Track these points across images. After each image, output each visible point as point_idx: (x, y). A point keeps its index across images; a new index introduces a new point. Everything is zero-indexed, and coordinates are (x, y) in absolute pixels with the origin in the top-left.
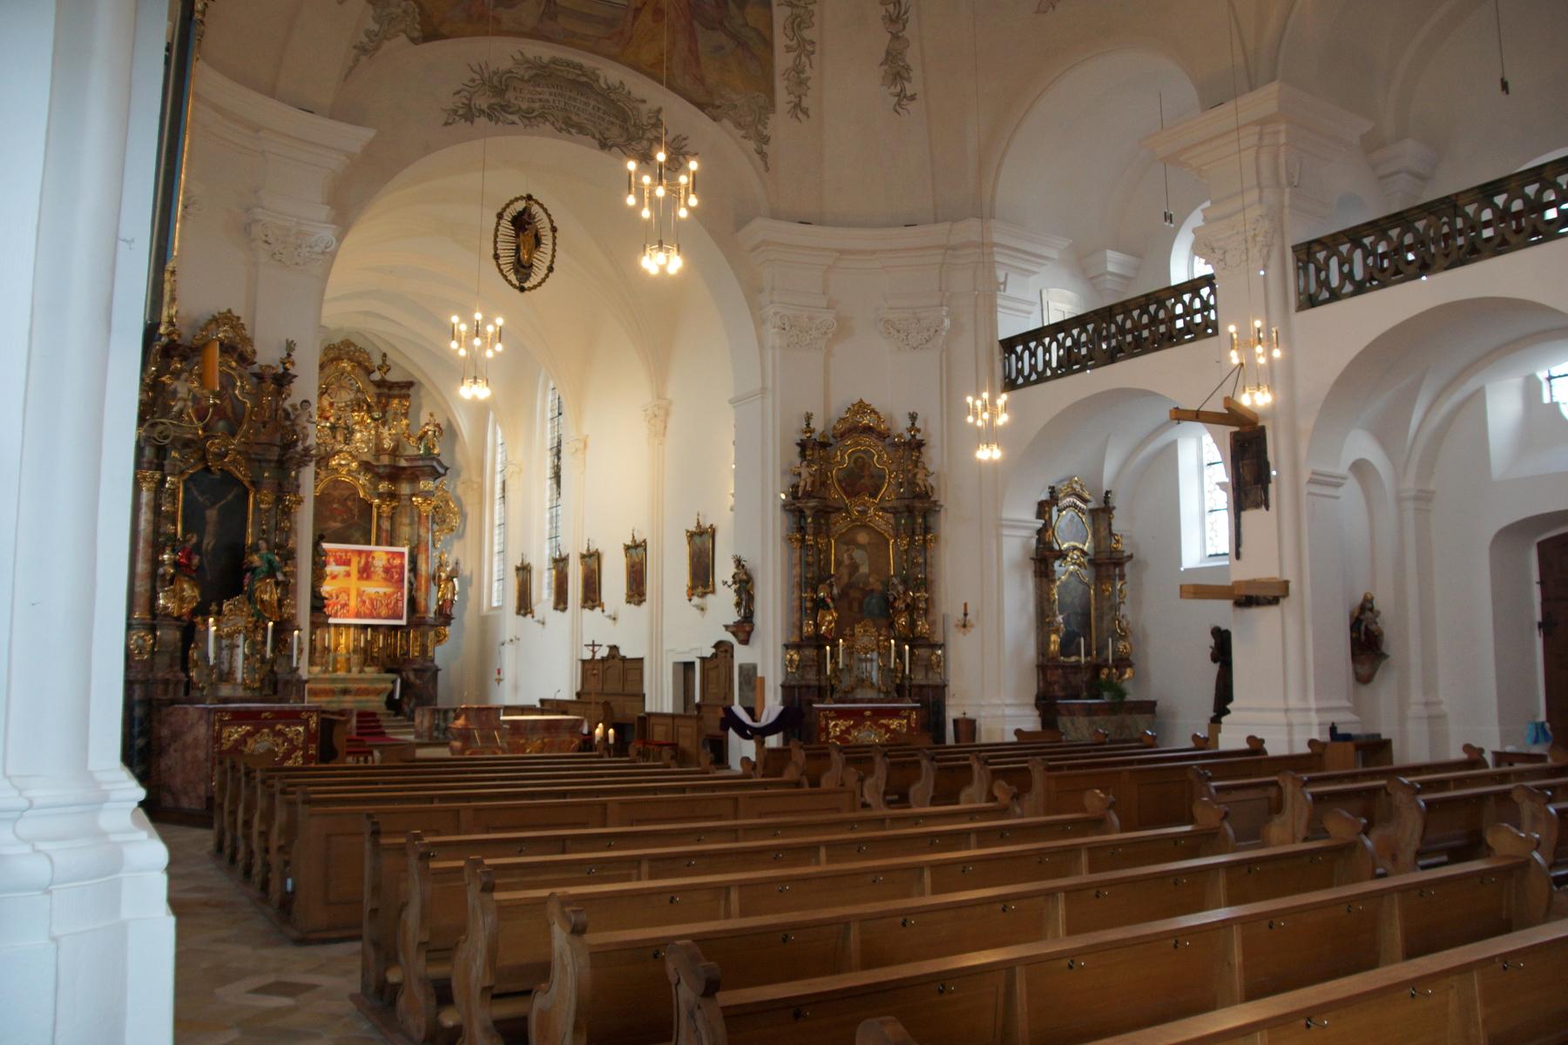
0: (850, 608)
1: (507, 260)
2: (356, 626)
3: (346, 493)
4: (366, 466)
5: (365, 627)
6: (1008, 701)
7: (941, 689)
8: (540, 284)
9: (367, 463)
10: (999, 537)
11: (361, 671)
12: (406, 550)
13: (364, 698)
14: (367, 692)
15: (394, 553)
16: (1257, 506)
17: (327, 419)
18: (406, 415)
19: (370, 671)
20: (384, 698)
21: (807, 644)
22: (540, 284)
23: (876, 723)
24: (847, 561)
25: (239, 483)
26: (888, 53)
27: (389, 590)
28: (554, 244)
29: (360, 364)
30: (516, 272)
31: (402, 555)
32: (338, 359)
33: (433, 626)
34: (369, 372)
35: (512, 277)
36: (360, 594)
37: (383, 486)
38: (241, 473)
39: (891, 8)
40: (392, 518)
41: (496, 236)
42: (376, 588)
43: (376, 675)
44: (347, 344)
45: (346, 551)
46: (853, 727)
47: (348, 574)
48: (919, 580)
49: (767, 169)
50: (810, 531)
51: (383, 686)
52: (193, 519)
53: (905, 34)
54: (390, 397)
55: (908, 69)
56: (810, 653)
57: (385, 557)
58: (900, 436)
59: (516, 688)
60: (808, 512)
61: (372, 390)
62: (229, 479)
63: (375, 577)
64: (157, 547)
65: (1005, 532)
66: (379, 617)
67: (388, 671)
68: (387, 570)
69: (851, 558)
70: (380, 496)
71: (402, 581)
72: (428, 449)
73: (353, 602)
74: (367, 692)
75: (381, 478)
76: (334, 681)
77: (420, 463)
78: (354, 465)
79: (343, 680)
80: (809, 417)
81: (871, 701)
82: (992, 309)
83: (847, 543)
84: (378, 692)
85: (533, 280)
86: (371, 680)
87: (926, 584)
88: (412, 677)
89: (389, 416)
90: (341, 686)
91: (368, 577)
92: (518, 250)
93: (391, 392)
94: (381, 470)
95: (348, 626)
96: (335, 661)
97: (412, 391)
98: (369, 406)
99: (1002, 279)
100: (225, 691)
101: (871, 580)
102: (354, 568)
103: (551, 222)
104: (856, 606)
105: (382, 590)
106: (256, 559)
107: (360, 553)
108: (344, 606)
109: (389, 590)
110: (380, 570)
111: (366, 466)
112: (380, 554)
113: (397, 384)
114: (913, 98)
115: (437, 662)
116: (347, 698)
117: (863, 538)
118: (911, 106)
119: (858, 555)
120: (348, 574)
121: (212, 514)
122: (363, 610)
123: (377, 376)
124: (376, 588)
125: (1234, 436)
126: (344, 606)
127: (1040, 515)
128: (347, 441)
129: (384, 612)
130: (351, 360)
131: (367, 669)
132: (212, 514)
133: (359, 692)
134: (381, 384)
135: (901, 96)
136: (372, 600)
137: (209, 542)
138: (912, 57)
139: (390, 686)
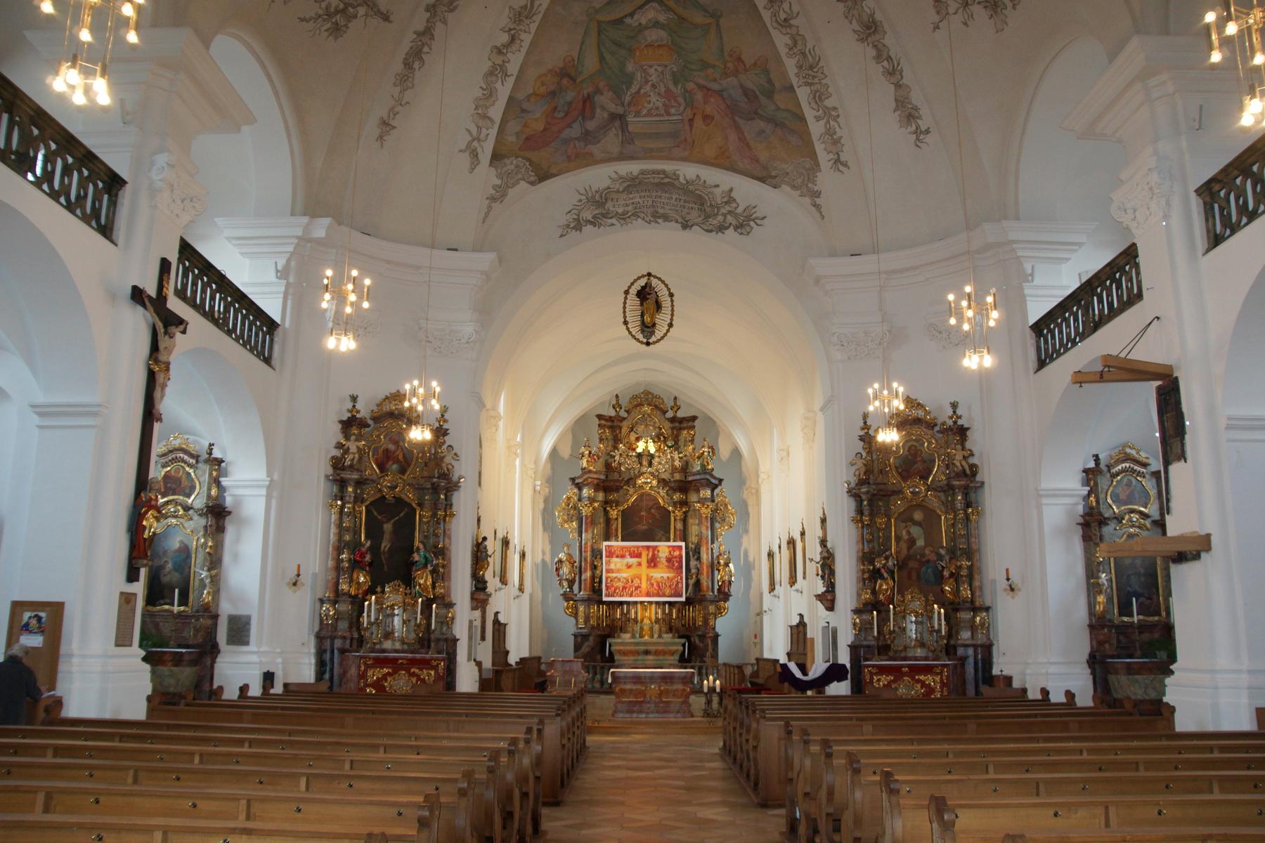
1: (635, 327)
2: (657, 603)
3: (651, 503)
4: (663, 482)
5: (664, 603)
6: (1052, 660)
8: (662, 338)
10: (1039, 507)
11: (660, 636)
16: (1179, 460)
18: (692, 441)
19: (667, 637)
20: (677, 657)
21: (871, 607)
22: (662, 338)
23: (913, 678)
24: (905, 537)
25: (410, 505)
26: (896, 100)
27: (671, 575)
28: (672, 306)
29: (656, 406)
30: (643, 331)
32: (641, 405)
33: (712, 602)
34: (665, 412)
35: (640, 337)
36: (649, 578)
37: (677, 497)
38: (410, 496)
39: (885, 64)
40: (685, 521)
41: (624, 308)
42: (661, 574)
44: (647, 393)
46: (894, 681)
47: (640, 564)
48: (966, 552)
49: (823, 217)
50: (866, 513)
52: (374, 530)
53: (904, 81)
54: (681, 429)
55: (916, 109)
57: (667, 550)
58: (944, 424)
59: (771, 649)
60: (864, 497)
61: (668, 425)
62: (400, 502)
63: (660, 565)
64: (339, 550)
65: (1044, 501)
66: (664, 595)
67: (680, 637)
68: (669, 560)
69: (909, 533)
70: (675, 504)
72: (703, 466)
73: (644, 585)
75: (675, 490)
76: (637, 644)
77: (698, 477)
78: (655, 483)
79: (645, 644)
82: (1022, 300)
84: (672, 653)
85: (658, 334)
86: (666, 644)
87: (970, 553)
89: (681, 443)
90: (642, 648)
91: (655, 566)
92: (642, 316)
93: (679, 425)
95: (650, 603)
96: (642, 628)
97: (697, 423)
99: (1029, 271)
100: (388, 645)
101: (927, 552)
102: (644, 560)
103: (669, 289)
105: (665, 575)
106: (416, 557)
107: (648, 548)
109: (671, 575)
110: (664, 560)
112: (663, 548)
114: (927, 132)
115: (717, 630)
116: (650, 657)
117: (918, 516)
118: (928, 138)
120: (640, 564)
121: (388, 527)
122: (651, 590)
123: (670, 414)
124: (661, 574)
125: (1159, 389)
126: (637, 588)
127: (1086, 482)
128: (650, 464)
129: (668, 591)
130: (649, 405)
131: (665, 636)
132: (388, 527)
134: (673, 420)
135: (918, 132)
137: (385, 545)
138: (916, 98)
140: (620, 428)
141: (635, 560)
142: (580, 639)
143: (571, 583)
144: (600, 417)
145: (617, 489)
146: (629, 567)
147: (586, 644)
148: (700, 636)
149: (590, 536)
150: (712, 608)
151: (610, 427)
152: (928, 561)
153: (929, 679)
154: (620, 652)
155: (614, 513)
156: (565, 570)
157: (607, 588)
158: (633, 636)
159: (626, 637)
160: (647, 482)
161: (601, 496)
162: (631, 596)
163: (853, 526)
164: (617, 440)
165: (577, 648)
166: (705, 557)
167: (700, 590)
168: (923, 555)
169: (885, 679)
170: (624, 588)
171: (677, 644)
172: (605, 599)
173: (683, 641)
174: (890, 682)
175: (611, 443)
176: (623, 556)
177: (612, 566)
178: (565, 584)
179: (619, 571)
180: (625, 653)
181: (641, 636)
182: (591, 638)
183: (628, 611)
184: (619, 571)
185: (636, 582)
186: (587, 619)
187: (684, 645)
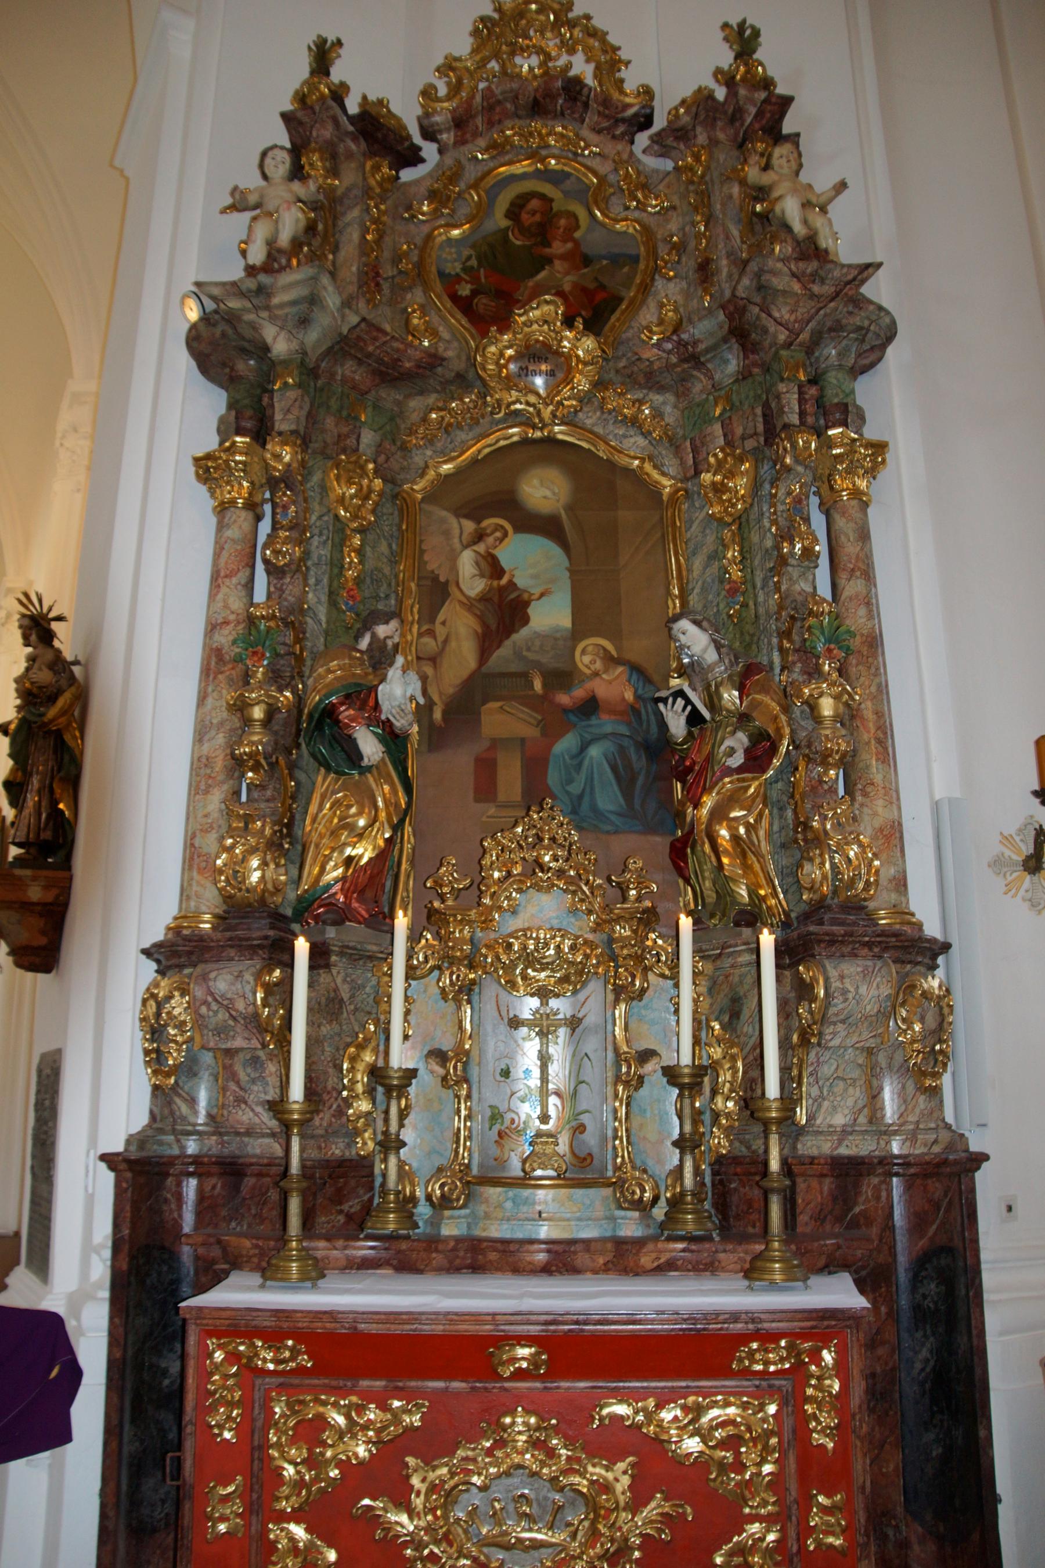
0: (486, 788)
7: (948, 1178)
24: (470, 579)
56: (235, 983)
80: (323, 56)
81: (563, 1260)
83: (475, 510)
101: (585, 659)
104: (510, 778)
117: (543, 490)
119: (528, 558)
152: (590, 706)
153: (692, 1424)
163: (200, 502)
168: (562, 677)
169: (354, 1429)
174: (392, 1451)
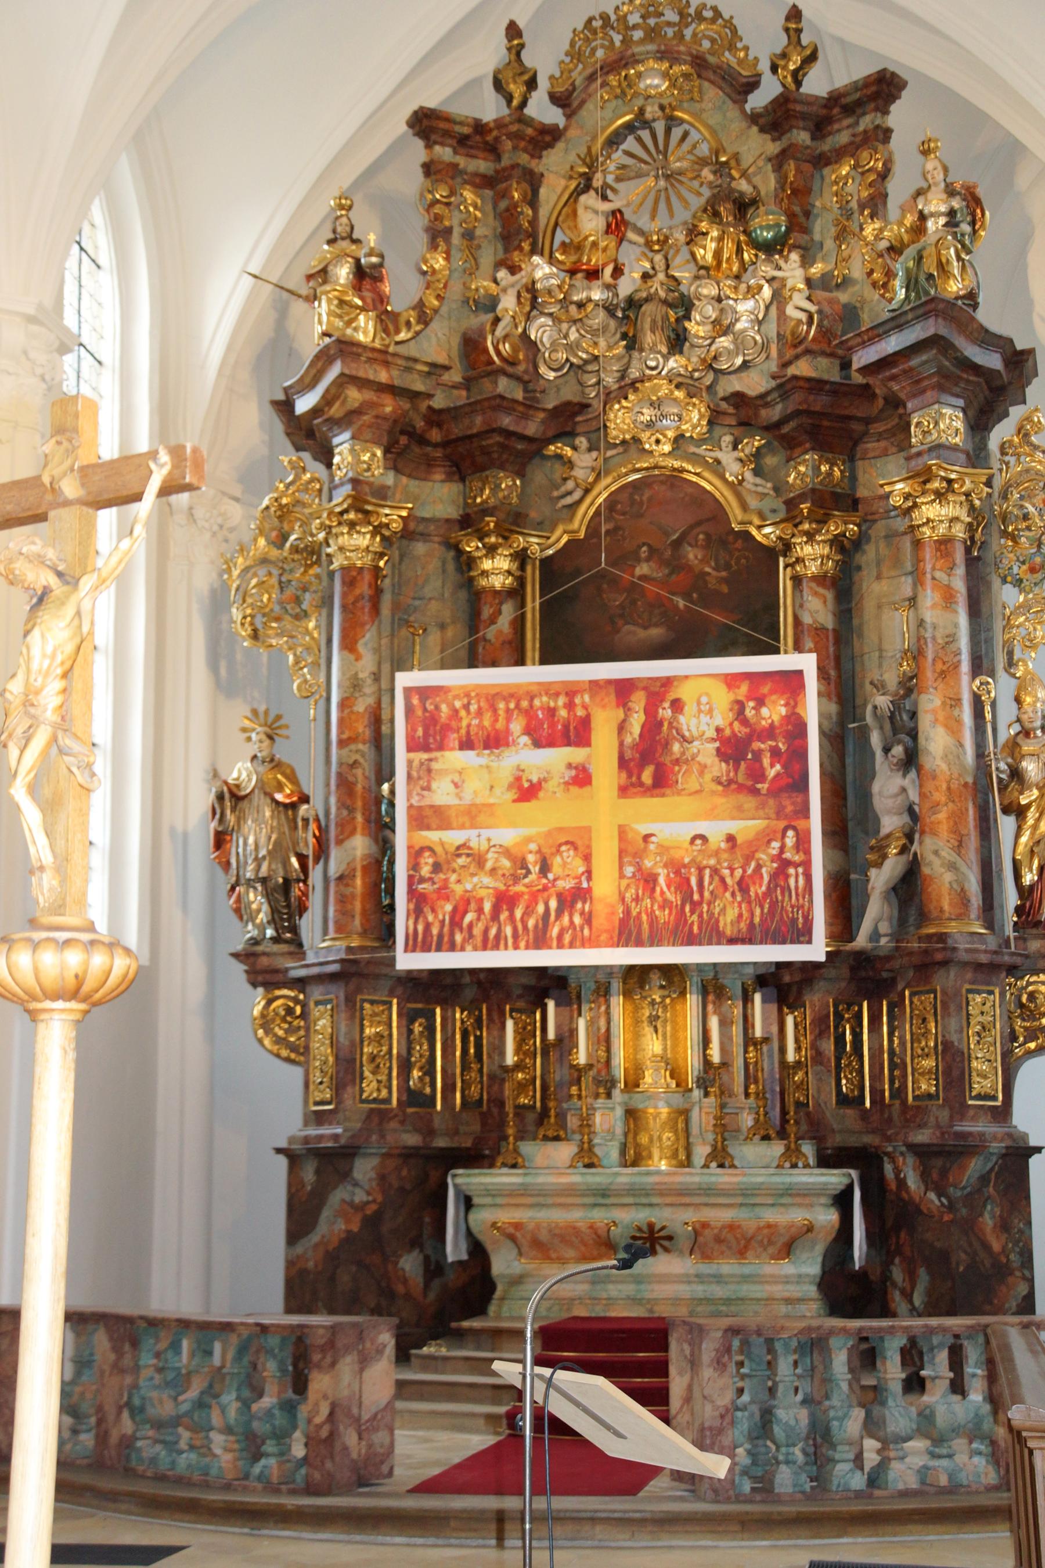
2: (713, 984)
3: (677, 523)
4: (738, 413)
9: (738, 399)
11: (720, 1157)
12: (807, 663)
13: (728, 1267)
14: (738, 1242)
15: (755, 678)
17: (593, 274)
19: (759, 1160)
20: (809, 1265)
29: (699, 63)
31: (793, 681)
33: (990, 970)
36: (630, 848)
37: (804, 471)
40: (842, 585)
42: (695, 822)
43: (760, 1177)
45: (571, 691)
47: (582, 777)
51: (797, 1216)
54: (822, 161)
57: (722, 698)
61: (755, 147)
66: (713, 935)
67: (825, 1161)
68: (733, 748)
71: (801, 785)
73: (605, 886)
74: (738, 1242)
76: (603, 1195)
77: (893, 344)
86: (747, 1196)
88: (913, 1182)
89: (822, 229)
91: (662, 783)
94: (775, 413)
97: (901, 116)
98: (743, 207)
102: (602, 754)
105: (717, 830)
107: (623, 689)
108: (575, 896)
109: (745, 828)
110: (706, 752)
111: (738, 413)
112: (705, 688)
113: (834, 99)
120: (582, 777)
124: (695, 822)
126: (570, 899)
128: (678, 342)
129: (729, 913)
133: (703, 1242)
134: (776, 119)
136: (677, 869)
139: (830, 1217)
140: (533, 181)
141: (556, 759)
142: (315, 1167)
143: (286, 902)
144: (426, 124)
145: (523, 454)
146: (527, 791)
147: (338, 1196)
148: (922, 1153)
149: (366, 665)
150: (986, 1007)
151: (484, 182)
154: (512, 1235)
155: (496, 570)
156: (255, 835)
157: (419, 902)
158: (587, 1158)
159: (551, 1161)
160: (659, 423)
161: (439, 498)
162: (540, 941)
164: (516, 237)
165: (301, 1215)
166: (945, 745)
167: (923, 917)
170: (504, 901)
171: (804, 1194)
172: (407, 961)
173: (835, 1178)
175: (488, 256)
176: (495, 741)
177: (442, 793)
178: (256, 899)
179: (473, 815)
180: (541, 1246)
181: (633, 1156)
182: (364, 1169)
183: (566, 1040)
184: (473, 815)
185: (566, 868)
186: (347, 1070)
187: (842, 1201)
